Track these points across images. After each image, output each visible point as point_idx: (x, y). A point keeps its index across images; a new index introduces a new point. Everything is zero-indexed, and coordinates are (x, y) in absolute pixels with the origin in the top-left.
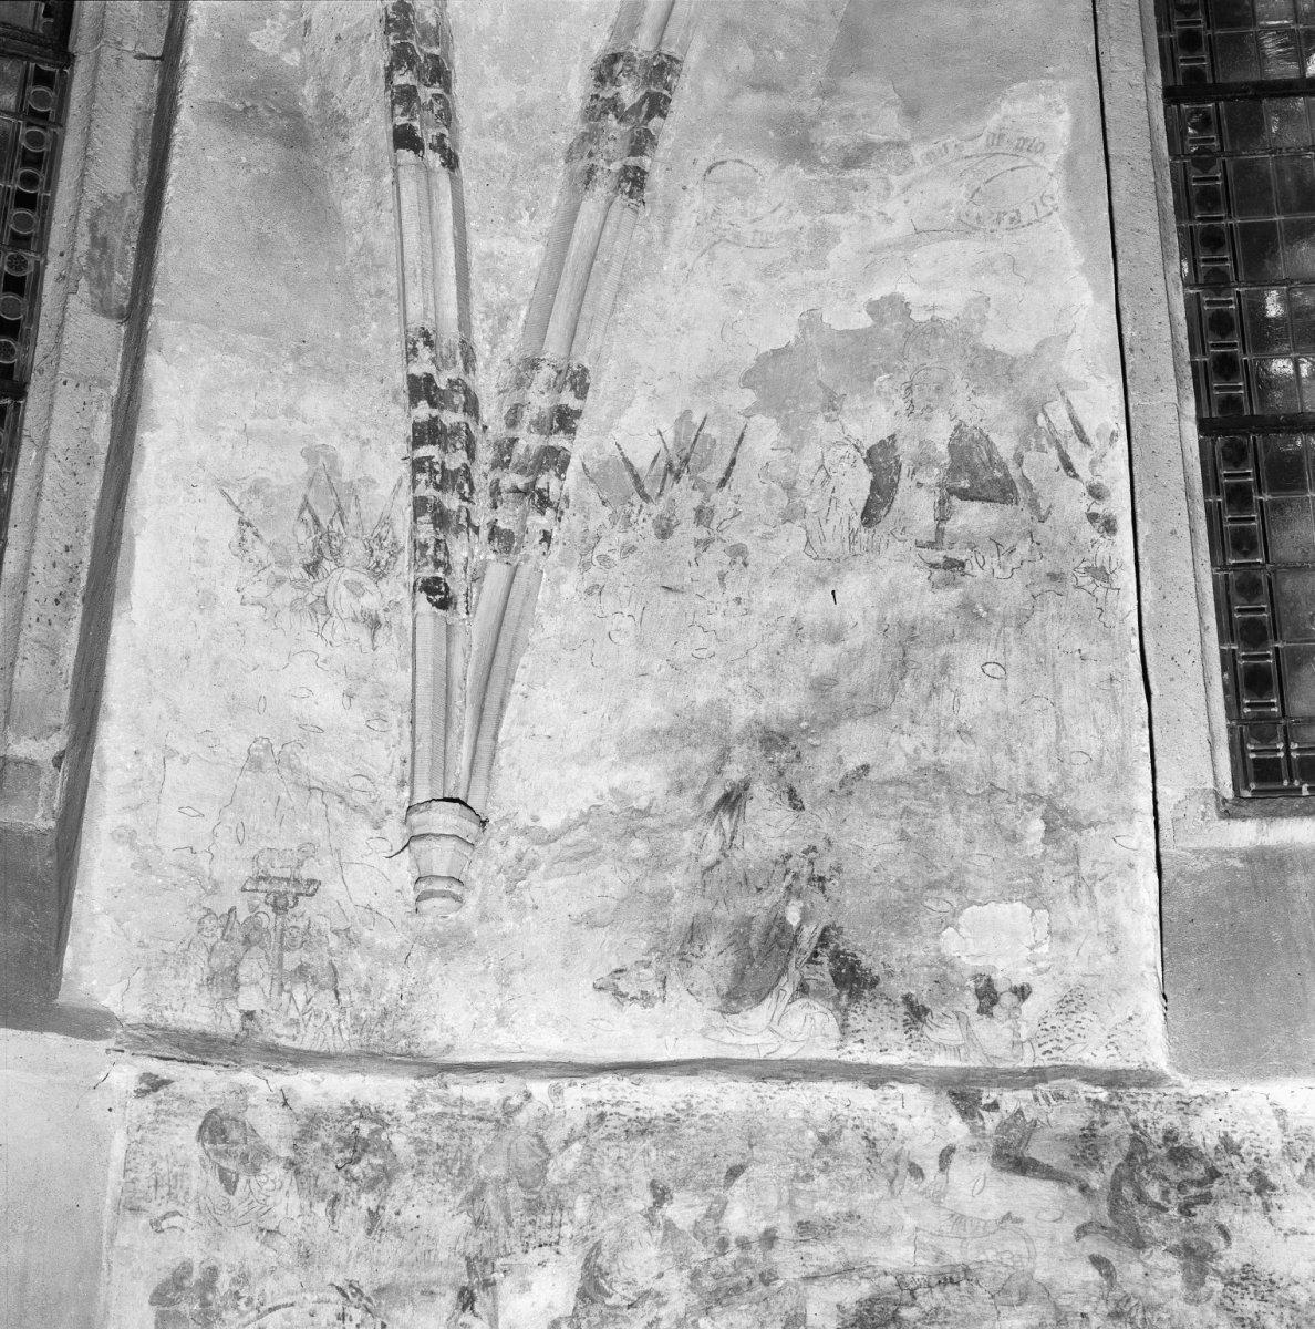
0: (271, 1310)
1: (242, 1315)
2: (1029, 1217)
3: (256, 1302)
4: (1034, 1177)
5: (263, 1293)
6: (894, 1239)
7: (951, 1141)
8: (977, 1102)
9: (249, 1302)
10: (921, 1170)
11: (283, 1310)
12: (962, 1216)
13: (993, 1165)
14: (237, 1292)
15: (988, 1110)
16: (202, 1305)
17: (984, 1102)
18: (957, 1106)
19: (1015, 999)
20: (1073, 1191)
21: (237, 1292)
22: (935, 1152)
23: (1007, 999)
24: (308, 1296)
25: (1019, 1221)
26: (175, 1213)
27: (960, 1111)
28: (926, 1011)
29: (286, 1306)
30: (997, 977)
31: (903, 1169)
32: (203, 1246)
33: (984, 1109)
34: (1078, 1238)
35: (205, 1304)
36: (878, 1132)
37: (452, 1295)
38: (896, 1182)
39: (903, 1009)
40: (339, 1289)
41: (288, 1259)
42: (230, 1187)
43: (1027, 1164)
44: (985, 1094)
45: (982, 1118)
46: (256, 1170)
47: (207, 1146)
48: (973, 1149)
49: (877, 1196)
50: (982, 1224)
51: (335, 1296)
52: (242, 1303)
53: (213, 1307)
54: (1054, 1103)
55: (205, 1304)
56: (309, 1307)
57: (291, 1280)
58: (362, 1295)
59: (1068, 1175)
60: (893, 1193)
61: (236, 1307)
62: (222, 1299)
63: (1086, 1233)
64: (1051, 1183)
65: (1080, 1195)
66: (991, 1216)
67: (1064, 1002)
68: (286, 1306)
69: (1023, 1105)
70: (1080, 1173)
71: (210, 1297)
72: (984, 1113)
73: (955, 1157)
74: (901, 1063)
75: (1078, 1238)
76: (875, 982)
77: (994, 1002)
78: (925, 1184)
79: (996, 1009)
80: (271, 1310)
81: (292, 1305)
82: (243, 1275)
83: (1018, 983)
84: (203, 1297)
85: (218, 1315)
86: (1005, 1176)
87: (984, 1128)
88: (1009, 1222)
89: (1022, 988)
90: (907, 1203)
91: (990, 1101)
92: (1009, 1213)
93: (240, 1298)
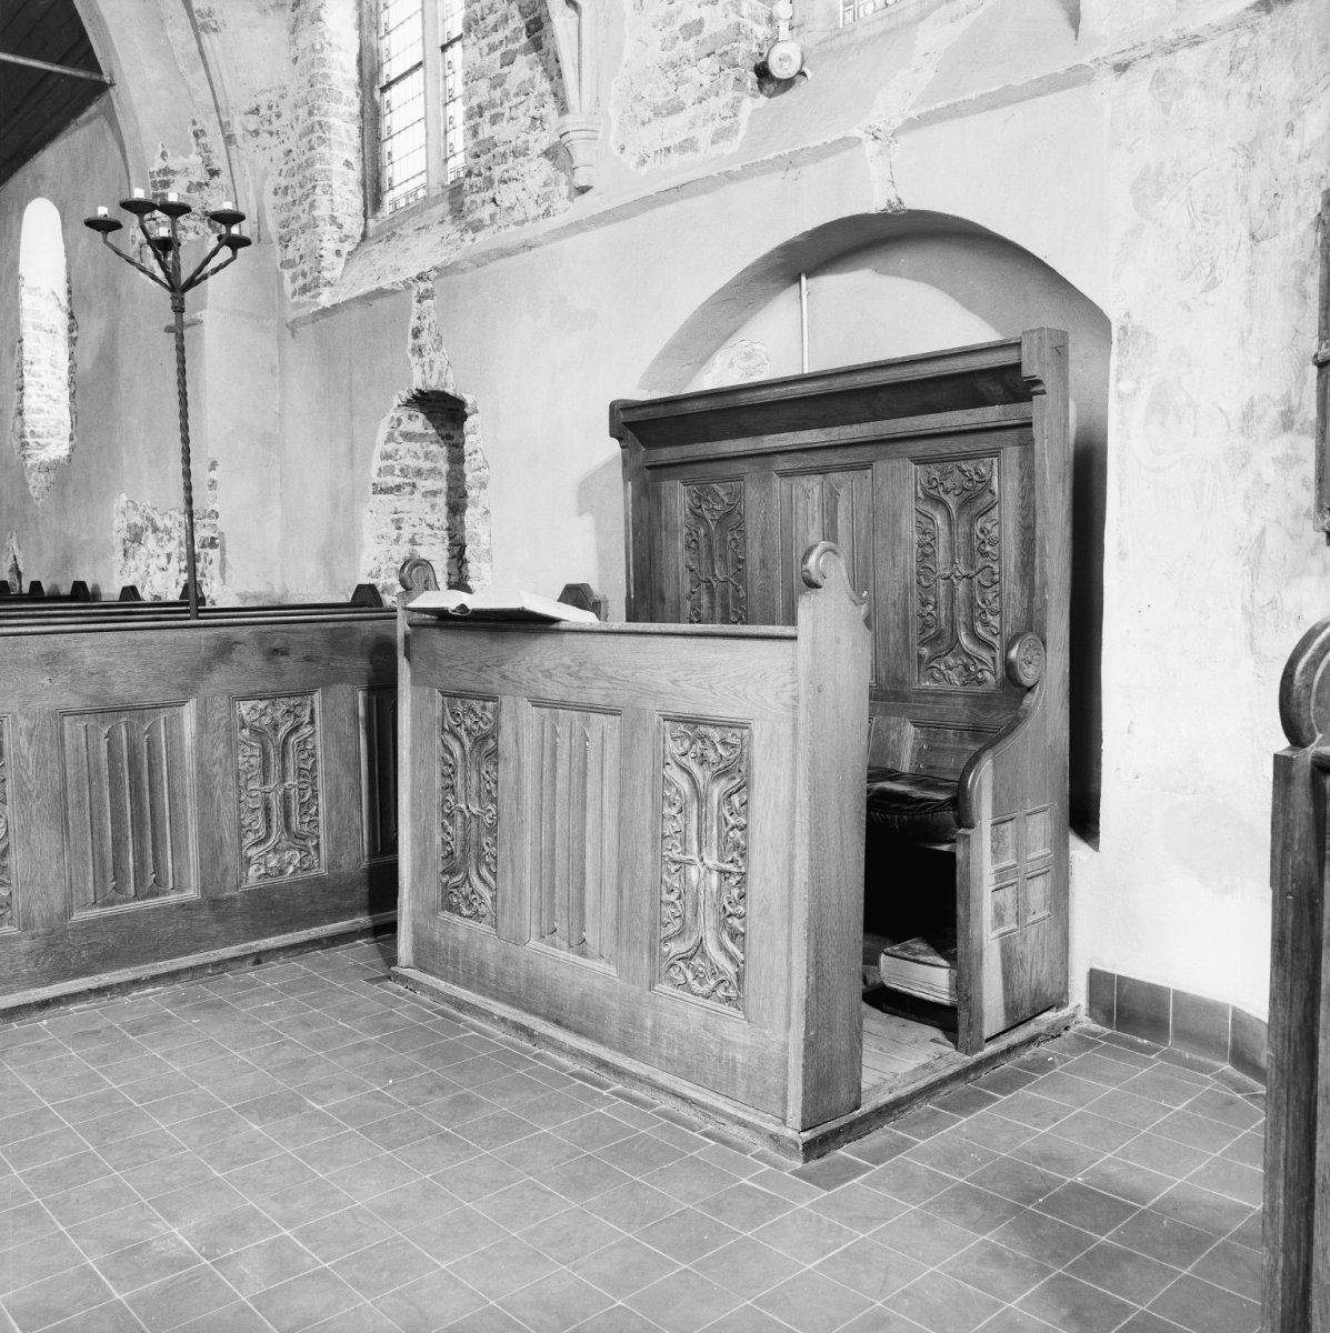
26: (1139, 139)
37: (1282, 128)
40: (1234, 149)
42: (1166, 110)
46: (1181, 95)
47: (1155, 92)
51: (1231, 152)
61: (1175, 181)
71: (1160, 179)
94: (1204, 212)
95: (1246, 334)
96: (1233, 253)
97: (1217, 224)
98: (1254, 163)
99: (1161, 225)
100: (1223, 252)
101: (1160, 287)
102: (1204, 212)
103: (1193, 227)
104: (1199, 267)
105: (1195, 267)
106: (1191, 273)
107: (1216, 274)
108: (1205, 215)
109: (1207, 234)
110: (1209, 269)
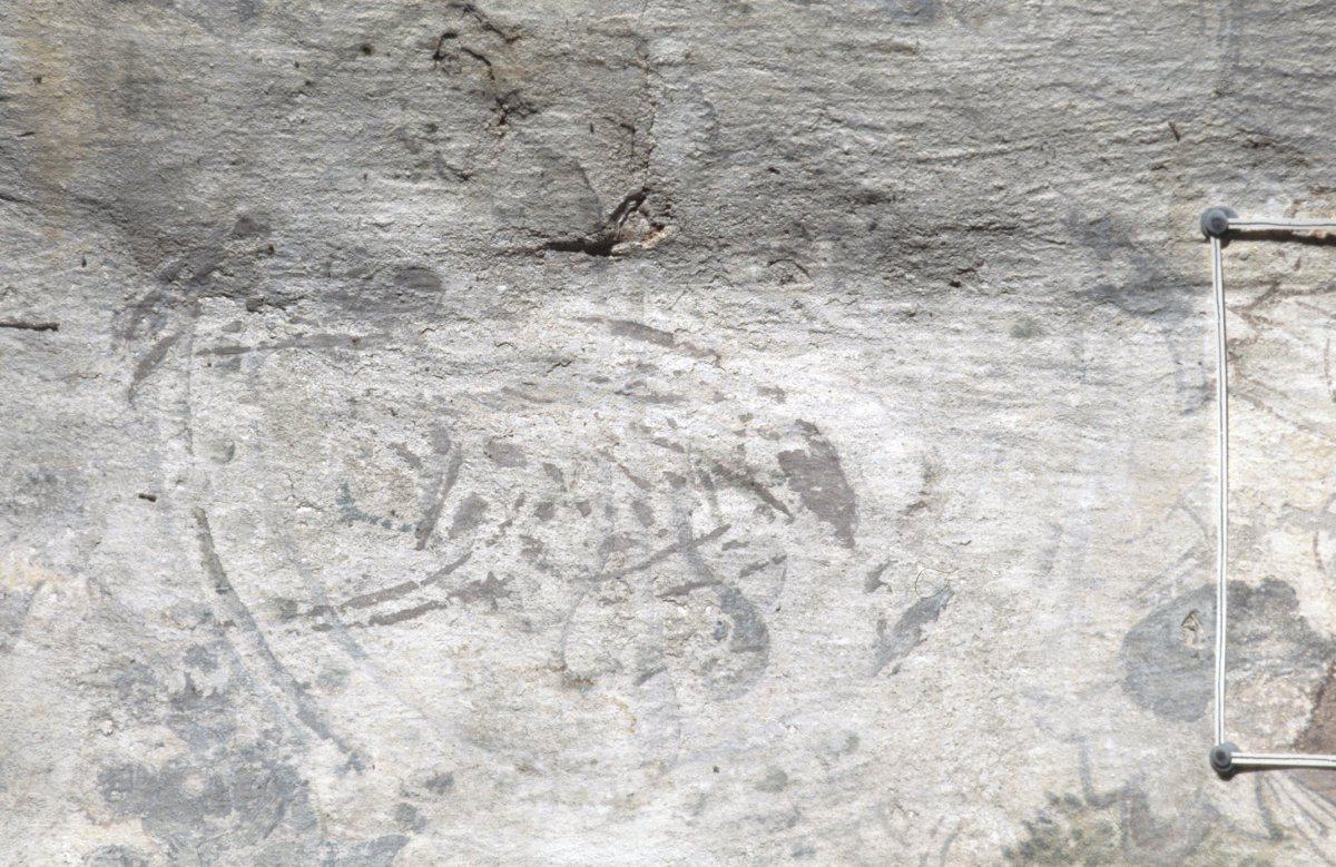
0: (223, 588)
1: (241, 681)
3: (203, 637)
5: (172, 617)
9: (200, 658)
11: (220, 548)
14: (176, 701)
16: (223, 809)
21: (176, 701)
24: (171, 468)
29: (205, 538)
32: (36, 825)
35: (218, 798)
40: (145, 368)
41: (63, 541)
51: (165, 386)
52: (206, 682)
53: (225, 770)
55: (218, 798)
56: (202, 461)
57: (127, 528)
58: (155, 298)
61: (220, 699)
62: (196, 740)
68: (205, 538)
71: (195, 785)
80: (223, 588)
81: (203, 521)
82: (123, 685)
84: (196, 809)
85: (248, 753)
93: (192, 690)
94: (425, 531)
95: (1119, 271)
96: (671, 361)
97: (501, 453)
98: (246, 227)
99: (441, 784)
100: (655, 415)
101: (778, 782)
102: (425, 531)
103: (489, 591)
104: (708, 551)
105: (707, 577)
106: (731, 600)
107: (761, 454)
108: (444, 524)
109: (544, 511)
110: (735, 503)
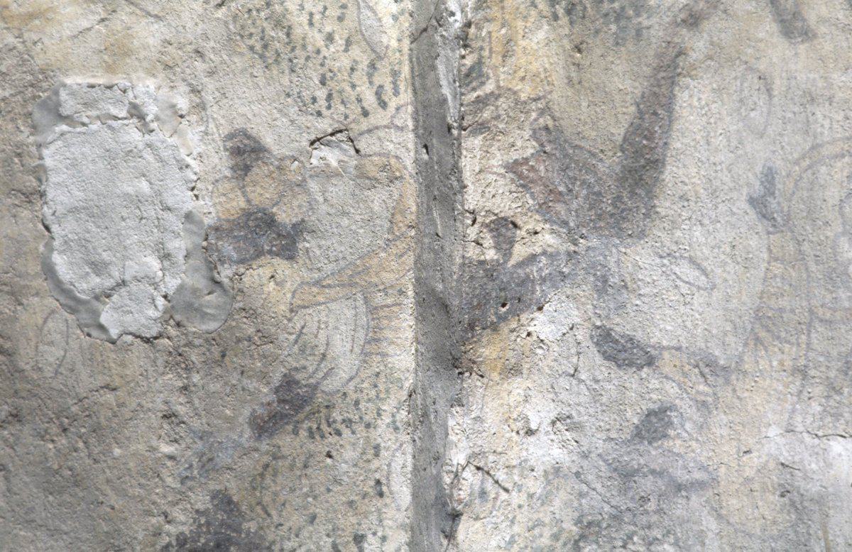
2: (759, 152)
4: (667, 130)
6: (814, 488)
7: (581, 334)
8: (490, 271)
10: (650, 413)
12: (759, 316)
13: (642, 235)
15: (512, 243)
17: (491, 254)
18: (503, 318)
19: (258, 171)
20: (698, 45)
22: (613, 380)
23: (262, 192)
25: (769, 177)
27: (516, 313)
28: (289, 382)
30: (210, 209)
31: (652, 455)
33: (507, 254)
34: (807, 35)
36: (562, 510)
38: (681, 476)
39: (287, 442)
43: (638, 153)
44: (472, 252)
45: (532, 258)
48: (603, 285)
49: (711, 524)
50: (777, 268)
54: (490, 87)
59: (659, 56)
60: (700, 485)
63: (796, 15)
64: (682, 97)
65: (706, 25)
66: (755, 243)
67: (265, 54)
69: (497, 160)
70: (656, 28)
72: (520, 251)
73: (621, 326)
74: (409, 449)
75: (807, 35)
76: (225, 501)
77: (269, 222)
78: (685, 405)
79: (285, 216)
83: (221, 162)
86: (664, 206)
87: (552, 256)
88: (773, 204)
89: (237, 152)
90: (729, 449)
91: (488, 241)
92: (752, 201)
